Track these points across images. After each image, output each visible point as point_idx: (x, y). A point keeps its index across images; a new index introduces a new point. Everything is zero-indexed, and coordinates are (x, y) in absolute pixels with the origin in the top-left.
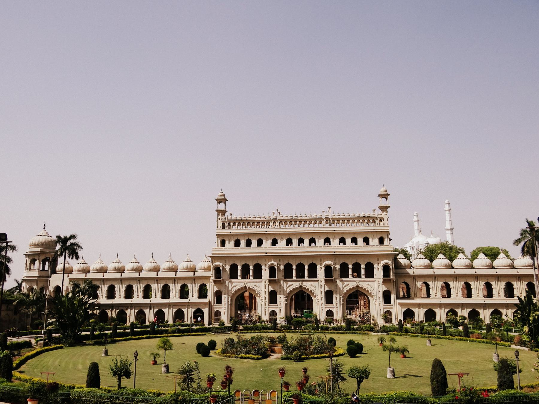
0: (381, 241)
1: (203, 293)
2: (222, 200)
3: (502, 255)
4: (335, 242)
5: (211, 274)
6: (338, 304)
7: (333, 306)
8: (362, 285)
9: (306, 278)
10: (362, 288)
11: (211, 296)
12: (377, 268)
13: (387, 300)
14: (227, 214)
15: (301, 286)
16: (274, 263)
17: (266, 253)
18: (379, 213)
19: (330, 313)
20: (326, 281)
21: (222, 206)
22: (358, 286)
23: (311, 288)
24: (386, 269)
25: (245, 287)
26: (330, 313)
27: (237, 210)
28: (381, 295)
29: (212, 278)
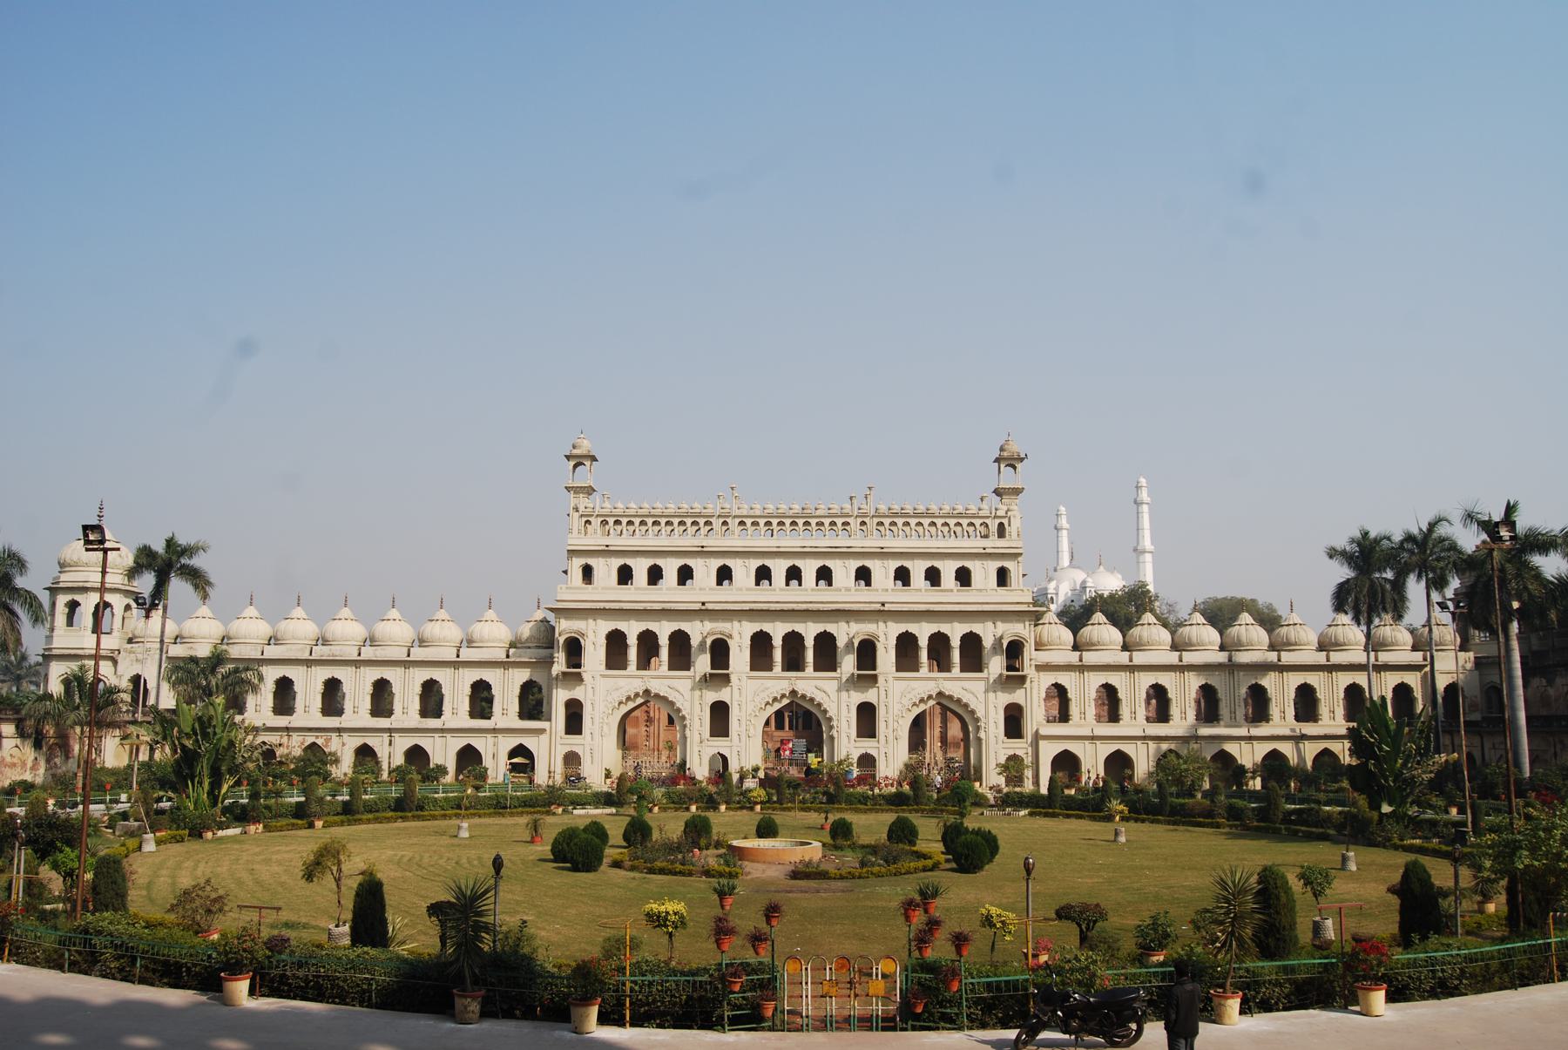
0: (1003, 577)
9: (810, 669)
10: (950, 697)
15: (794, 692)
22: (940, 694)
25: (647, 692)
26: (867, 761)
29: (560, 665)
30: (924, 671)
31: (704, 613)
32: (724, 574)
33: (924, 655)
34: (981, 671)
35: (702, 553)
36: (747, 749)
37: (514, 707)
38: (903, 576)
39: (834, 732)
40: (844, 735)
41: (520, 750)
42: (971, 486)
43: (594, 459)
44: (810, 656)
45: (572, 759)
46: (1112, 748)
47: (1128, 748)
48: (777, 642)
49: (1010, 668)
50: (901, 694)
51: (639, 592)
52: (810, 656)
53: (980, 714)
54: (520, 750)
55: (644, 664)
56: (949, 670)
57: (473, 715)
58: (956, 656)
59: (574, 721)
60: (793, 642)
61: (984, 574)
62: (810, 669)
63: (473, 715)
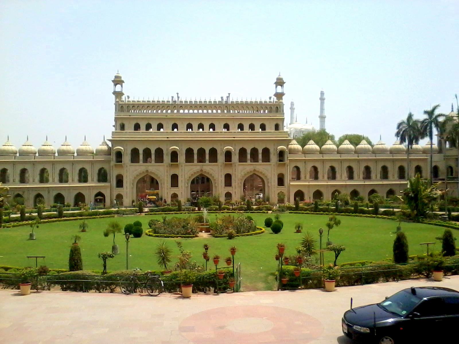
0: (277, 127)
2: (118, 81)
3: (364, 142)
4: (234, 128)
5: (113, 157)
6: (237, 186)
7: (231, 189)
9: (207, 162)
10: (258, 171)
12: (273, 154)
13: (281, 181)
14: (123, 98)
15: (202, 170)
17: (168, 138)
19: (228, 195)
20: (226, 165)
21: (118, 88)
22: (255, 170)
23: (211, 172)
27: (134, 93)
29: (113, 163)
30: (249, 162)
33: (249, 156)
34: (269, 162)
36: (184, 192)
38: (241, 127)
39: (216, 185)
40: (220, 186)
41: (100, 194)
42: (265, 94)
43: (123, 82)
44: (207, 157)
45: (119, 197)
49: (280, 161)
50: (241, 170)
52: (207, 157)
53: (268, 177)
54: (100, 194)
55: (145, 161)
56: (258, 162)
58: (260, 156)
59: (120, 183)
62: (207, 162)
63: (80, 181)
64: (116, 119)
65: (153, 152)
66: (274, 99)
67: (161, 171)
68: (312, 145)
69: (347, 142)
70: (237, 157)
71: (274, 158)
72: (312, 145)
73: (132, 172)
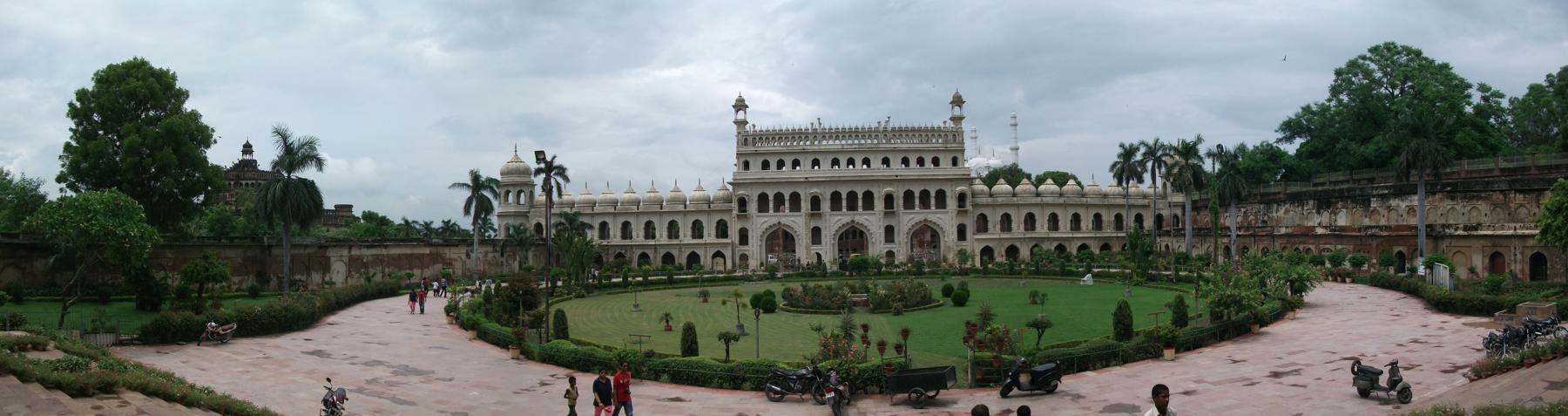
0: (955, 162)
1: (722, 230)
2: (740, 105)
4: (896, 163)
5: (735, 205)
8: (931, 217)
11: (734, 235)
16: (815, 190)
18: (950, 124)
21: (741, 115)
24: (962, 198)
26: (890, 254)
27: (760, 121)
28: (955, 230)
29: (735, 212)
31: (807, 182)
32: (816, 163)
33: (917, 202)
35: (804, 152)
36: (828, 251)
37: (714, 232)
42: (939, 118)
44: (860, 203)
45: (744, 257)
46: (1007, 245)
47: (1018, 244)
48: (844, 196)
50: (907, 220)
51: (773, 173)
52: (860, 203)
55: (777, 209)
57: (694, 237)
58: (933, 201)
60: (852, 196)
61: (945, 162)
63: (694, 237)
64: (739, 155)
65: (787, 197)
66: (950, 124)
67: (798, 223)
68: (1002, 187)
69: (1050, 181)
70: (901, 202)
71: (952, 204)
72: (1002, 187)
73: (760, 224)
